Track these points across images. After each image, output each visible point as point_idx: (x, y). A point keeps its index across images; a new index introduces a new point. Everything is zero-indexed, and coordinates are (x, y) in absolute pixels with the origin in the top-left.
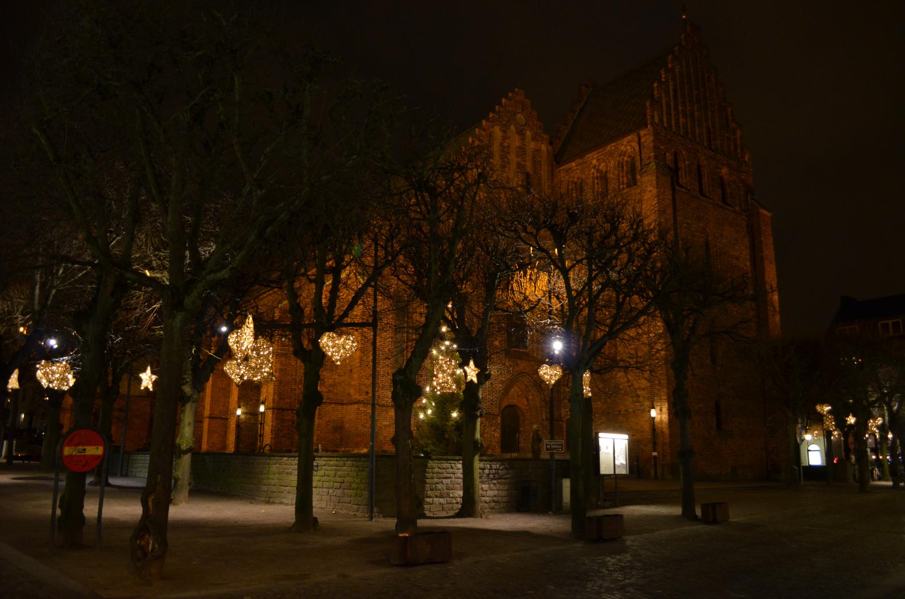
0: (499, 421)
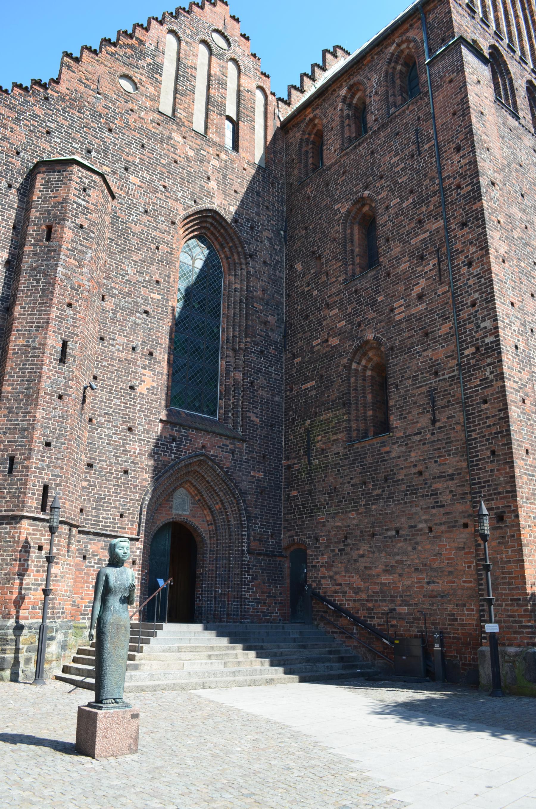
0: (138, 553)
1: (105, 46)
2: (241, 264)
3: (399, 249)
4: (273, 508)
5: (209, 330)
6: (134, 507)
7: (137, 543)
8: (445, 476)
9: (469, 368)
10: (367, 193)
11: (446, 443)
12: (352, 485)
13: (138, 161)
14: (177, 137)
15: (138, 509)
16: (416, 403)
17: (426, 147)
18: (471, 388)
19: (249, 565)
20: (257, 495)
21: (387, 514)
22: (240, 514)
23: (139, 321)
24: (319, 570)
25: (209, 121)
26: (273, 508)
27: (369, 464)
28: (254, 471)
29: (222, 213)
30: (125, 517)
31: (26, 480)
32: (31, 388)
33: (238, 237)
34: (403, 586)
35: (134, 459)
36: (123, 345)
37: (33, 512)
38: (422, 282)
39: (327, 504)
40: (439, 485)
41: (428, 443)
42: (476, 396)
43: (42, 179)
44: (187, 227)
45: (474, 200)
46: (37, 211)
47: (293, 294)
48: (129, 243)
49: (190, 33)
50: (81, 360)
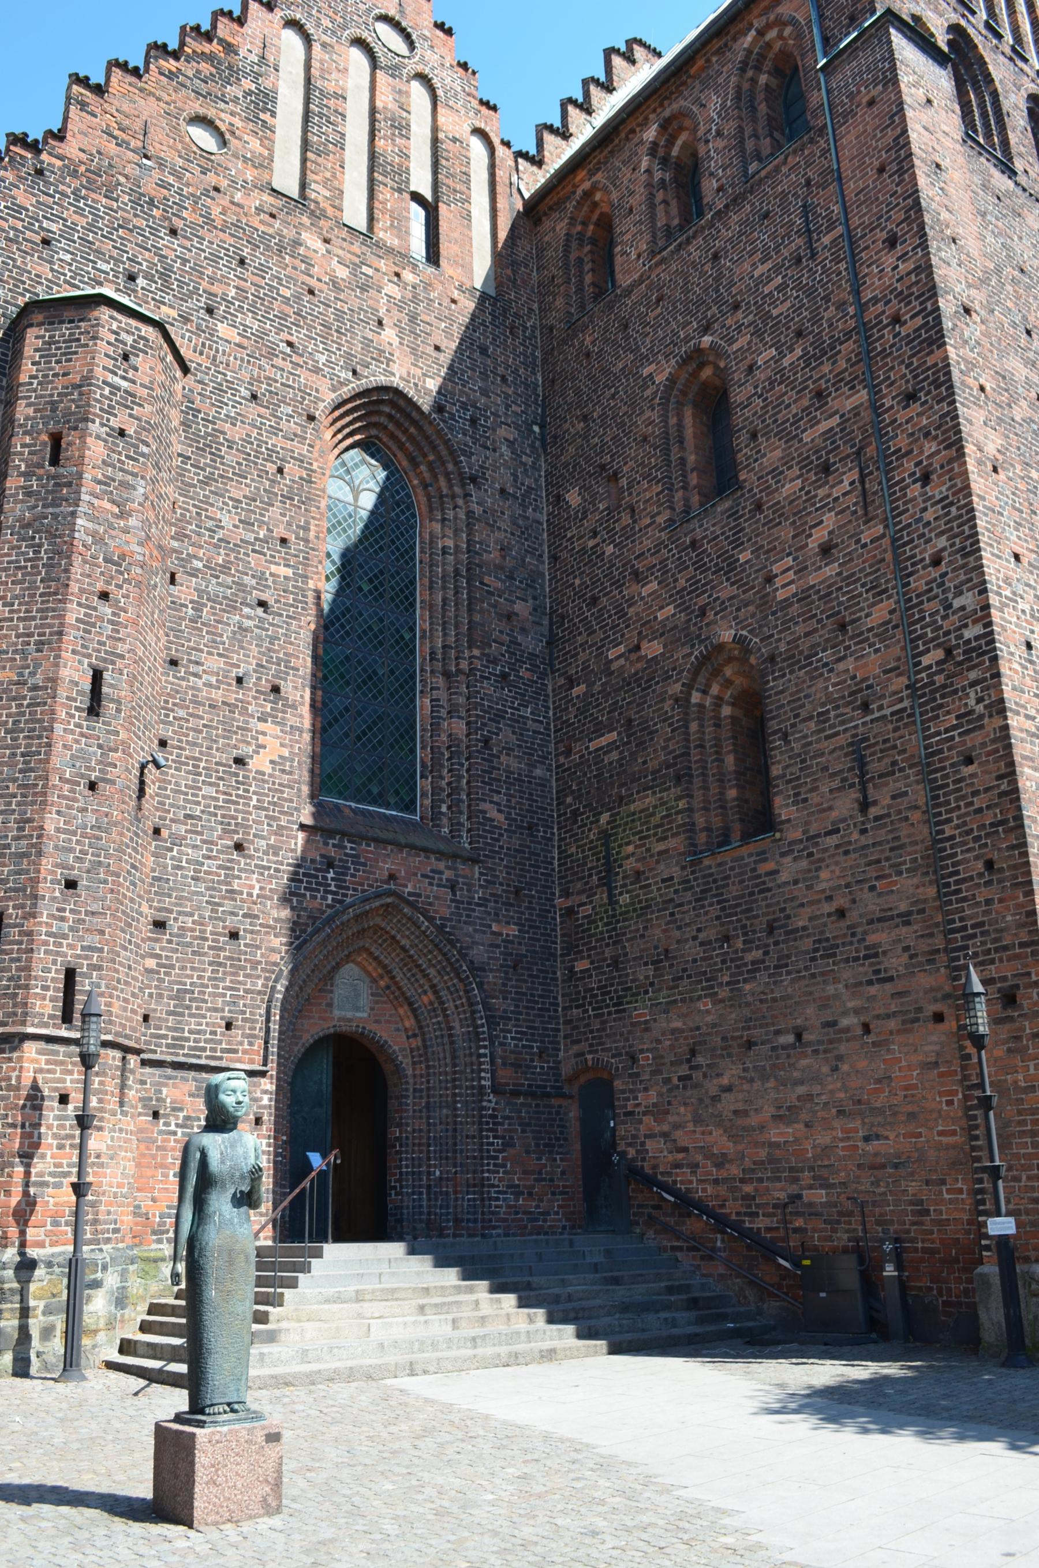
0: (265, 1100)
1: (156, 58)
2: (454, 496)
3: (778, 453)
4: (540, 996)
5: (393, 636)
6: (253, 1007)
7: (263, 1080)
8: (892, 918)
9: (932, 692)
10: (707, 340)
11: (892, 849)
12: (702, 944)
13: (232, 292)
14: (312, 241)
15: (263, 1011)
16: (825, 769)
17: (826, 240)
18: (939, 733)
19: (496, 1117)
20: (506, 973)
21: (774, 1000)
22: (473, 1012)
23: (248, 623)
24: (640, 1122)
25: (376, 204)
26: (540, 996)
27: (735, 898)
28: (498, 922)
29: (411, 393)
30: (238, 1028)
31: (29, 960)
32: (32, 770)
33: (447, 442)
34: (814, 1147)
35: (249, 909)
36: (218, 674)
37: (46, 1025)
38: (830, 520)
39: (652, 984)
40: (881, 937)
41: (855, 850)
42: (950, 749)
43: (37, 337)
44: (339, 424)
45: (930, 345)
46: (28, 405)
47: (564, 555)
48: (222, 464)
49: (330, 25)
50: (133, 708)
